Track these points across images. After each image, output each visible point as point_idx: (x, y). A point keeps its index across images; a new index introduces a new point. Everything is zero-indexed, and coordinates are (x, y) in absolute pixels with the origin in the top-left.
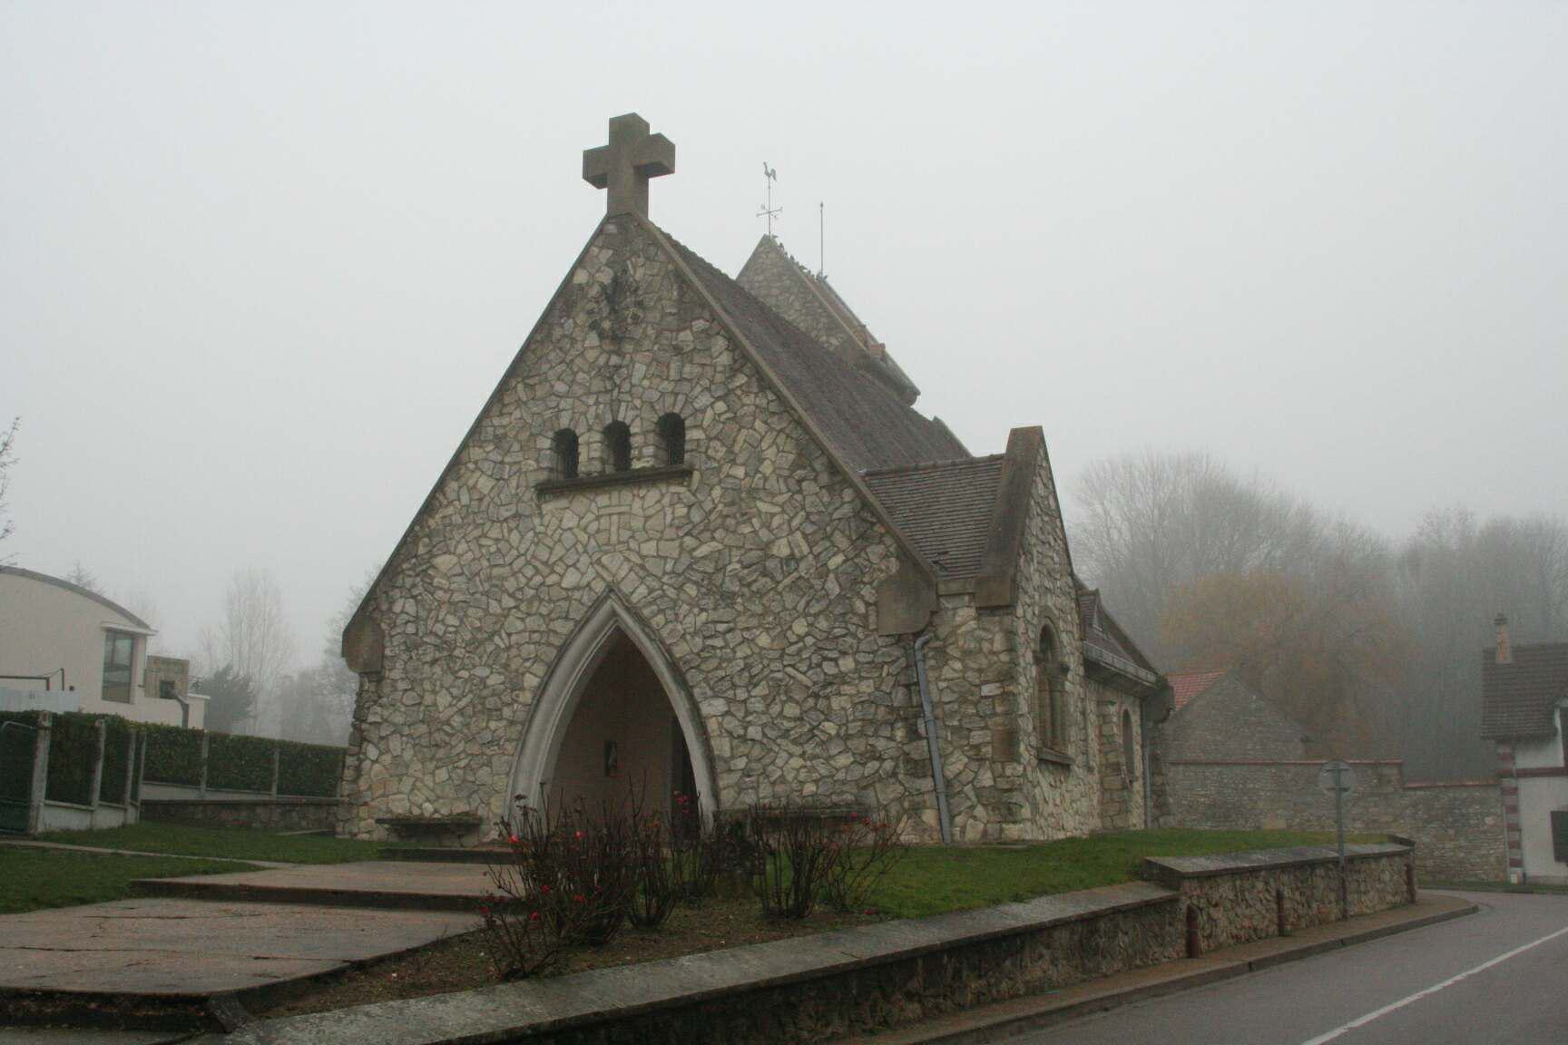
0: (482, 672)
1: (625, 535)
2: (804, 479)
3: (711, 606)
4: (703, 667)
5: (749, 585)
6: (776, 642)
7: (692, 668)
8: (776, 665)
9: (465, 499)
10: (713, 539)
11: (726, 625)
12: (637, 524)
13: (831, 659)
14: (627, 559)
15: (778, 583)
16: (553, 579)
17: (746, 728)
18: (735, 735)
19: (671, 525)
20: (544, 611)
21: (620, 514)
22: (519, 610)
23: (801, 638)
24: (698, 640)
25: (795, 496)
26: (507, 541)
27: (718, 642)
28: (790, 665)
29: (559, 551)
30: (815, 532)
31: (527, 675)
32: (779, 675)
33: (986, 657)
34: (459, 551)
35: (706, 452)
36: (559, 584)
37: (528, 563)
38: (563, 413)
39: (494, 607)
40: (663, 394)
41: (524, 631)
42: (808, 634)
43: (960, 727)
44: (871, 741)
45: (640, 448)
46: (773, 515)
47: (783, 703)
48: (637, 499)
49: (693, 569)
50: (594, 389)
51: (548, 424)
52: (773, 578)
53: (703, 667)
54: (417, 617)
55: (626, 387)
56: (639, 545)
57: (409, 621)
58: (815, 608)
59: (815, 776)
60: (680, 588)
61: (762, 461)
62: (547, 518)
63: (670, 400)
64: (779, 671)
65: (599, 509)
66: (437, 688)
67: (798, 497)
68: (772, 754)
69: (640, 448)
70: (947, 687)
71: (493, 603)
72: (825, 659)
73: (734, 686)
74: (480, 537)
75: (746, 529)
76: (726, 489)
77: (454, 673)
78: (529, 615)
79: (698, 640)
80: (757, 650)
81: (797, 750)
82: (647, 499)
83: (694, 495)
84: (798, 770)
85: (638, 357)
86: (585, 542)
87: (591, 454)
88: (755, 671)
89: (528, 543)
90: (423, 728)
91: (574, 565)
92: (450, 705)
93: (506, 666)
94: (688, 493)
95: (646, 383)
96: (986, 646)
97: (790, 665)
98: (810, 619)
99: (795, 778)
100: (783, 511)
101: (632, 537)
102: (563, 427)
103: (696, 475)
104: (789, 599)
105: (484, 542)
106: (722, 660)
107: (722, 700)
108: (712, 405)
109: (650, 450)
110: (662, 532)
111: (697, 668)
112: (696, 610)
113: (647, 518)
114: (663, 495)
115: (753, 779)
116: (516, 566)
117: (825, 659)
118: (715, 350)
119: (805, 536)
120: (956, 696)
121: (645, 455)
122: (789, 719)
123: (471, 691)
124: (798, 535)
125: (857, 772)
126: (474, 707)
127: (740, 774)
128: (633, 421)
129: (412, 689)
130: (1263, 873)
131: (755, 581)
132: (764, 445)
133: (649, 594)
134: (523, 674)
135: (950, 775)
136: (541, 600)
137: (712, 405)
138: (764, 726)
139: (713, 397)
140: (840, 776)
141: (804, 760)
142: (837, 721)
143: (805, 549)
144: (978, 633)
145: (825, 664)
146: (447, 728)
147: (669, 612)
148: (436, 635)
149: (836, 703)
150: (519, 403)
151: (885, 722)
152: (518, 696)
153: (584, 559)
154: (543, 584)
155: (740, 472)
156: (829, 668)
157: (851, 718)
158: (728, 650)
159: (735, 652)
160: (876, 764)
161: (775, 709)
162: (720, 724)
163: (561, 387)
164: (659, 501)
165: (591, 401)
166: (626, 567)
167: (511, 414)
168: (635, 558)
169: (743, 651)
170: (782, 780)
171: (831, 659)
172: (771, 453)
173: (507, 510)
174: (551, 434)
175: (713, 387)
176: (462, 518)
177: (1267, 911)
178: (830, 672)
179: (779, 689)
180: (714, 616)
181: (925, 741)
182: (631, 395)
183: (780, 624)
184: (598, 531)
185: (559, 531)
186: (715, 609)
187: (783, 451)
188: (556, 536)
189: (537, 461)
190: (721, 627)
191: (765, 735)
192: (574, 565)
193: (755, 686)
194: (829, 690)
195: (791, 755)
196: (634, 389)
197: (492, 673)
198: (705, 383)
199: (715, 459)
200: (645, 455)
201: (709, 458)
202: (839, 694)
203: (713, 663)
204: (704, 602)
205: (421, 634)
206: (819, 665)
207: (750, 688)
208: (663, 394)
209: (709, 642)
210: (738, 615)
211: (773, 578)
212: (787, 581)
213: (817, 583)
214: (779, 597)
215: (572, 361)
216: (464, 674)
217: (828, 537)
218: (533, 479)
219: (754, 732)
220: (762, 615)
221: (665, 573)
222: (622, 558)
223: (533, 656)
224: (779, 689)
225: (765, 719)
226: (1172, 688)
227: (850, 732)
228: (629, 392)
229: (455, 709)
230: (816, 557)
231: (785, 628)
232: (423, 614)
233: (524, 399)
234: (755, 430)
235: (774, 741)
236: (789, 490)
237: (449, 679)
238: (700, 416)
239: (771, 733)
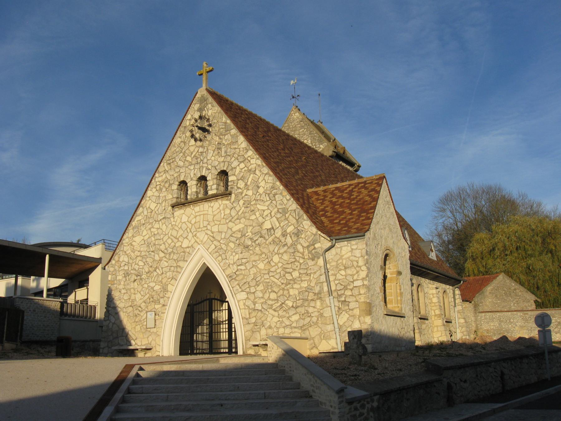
0: (152, 284)
1: (206, 223)
2: (276, 194)
3: (240, 252)
4: (237, 278)
5: (255, 241)
6: (266, 266)
7: (233, 279)
8: (266, 276)
9: (145, 213)
10: (240, 223)
11: (245, 260)
12: (210, 218)
13: (289, 273)
14: (206, 234)
15: (267, 240)
16: (178, 244)
17: (255, 305)
18: (251, 308)
19: (223, 218)
20: (175, 257)
21: (204, 214)
22: (166, 258)
23: (276, 264)
24: (235, 267)
25: (273, 202)
26: (161, 229)
27: (242, 267)
28: (272, 276)
29: (181, 232)
30: (281, 217)
31: (169, 285)
32: (268, 281)
33: (355, 268)
34: (143, 235)
35: (237, 186)
36: (181, 246)
37: (169, 238)
38: (182, 174)
39: (157, 258)
40: (219, 163)
41: (168, 266)
42: (279, 262)
43: (345, 301)
44: (306, 308)
45: (211, 186)
46: (264, 211)
47: (270, 293)
48: (210, 208)
49: (232, 236)
50: (193, 162)
51: (176, 179)
52: (264, 238)
53: (237, 278)
54: (128, 263)
55: (205, 160)
56: (211, 227)
57: (126, 265)
58: (282, 251)
59: (284, 325)
60: (227, 245)
61: (258, 187)
62: (176, 218)
63: (222, 164)
64: (268, 279)
65: (195, 213)
66: (136, 292)
67: (274, 202)
68: (266, 315)
69: (211, 186)
70: (339, 283)
71: (157, 255)
72: (287, 273)
73: (250, 287)
74: (151, 228)
75: (253, 217)
76: (245, 201)
77: (142, 286)
78: (170, 259)
79: (235, 267)
80: (258, 270)
81: (276, 314)
82: (216, 205)
83: (232, 204)
84: (276, 323)
85: (210, 148)
86: (190, 228)
87: (193, 188)
88: (257, 280)
89: (169, 229)
90: (131, 309)
91: (186, 238)
92: (141, 299)
93: (161, 282)
94: (230, 204)
95: (213, 158)
96: (355, 263)
97: (272, 276)
98: (280, 256)
99: (275, 326)
100: (268, 209)
101: (208, 224)
102: (181, 180)
103: (233, 195)
104: (271, 248)
105: (152, 230)
106: (244, 275)
107: (245, 292)
108: (239, 165)
109: (215, 187)
110: (220, 221)
111: (235, 279)
112: (234, 254)
113: (214, 216)
114: (220, 205)
115: (258, 327)
116: (164, 240)
117: (287, 273)
118: (239, 142)
119: (277, 219)
120: (343, 287)
121: (213, 188)
122: (272, 300)
123: (148, 293)
124: (274, 219)
125: (301, 323)
126: (150, 299)
127: (253, 325)
128: (208, 174)
129: (127, 293)
130: (493, 364)
131: (257, 240)
132: (260, 181)
133: (215, 248)
134: (167, 285)
135: (341, 323)
136: (174, 253)
137: (239, 165)
138: (262, 303)
139: (239, 162)
140: (294, 325)
141: (279, 318)
142: (292, 300)
143: (278, 225)
144: (351, 258)
145: (287, 275)
146: (140, 309)
147: (223, 255)
148: (135, 270)
149: (292, 292)
150: (165, 171)
151: (312, 300)
152: (166, 294)
153: (190, 235)
154: (175, 246)
155: (250, 193)
156: (288, 277)
157: (298, 298)
158: (247, 271)
159: (250, 272)
160: (309, 319)
161: (266, 296)
162: (244, 304)
163: (181, 163)
164: (219, 208)
165: (192, 167)
166: (206, 236)
167: (162, 176)
168: (209, 232)
169: (254, 270)
170: (270, 327)
171: (289, 273)
172: (262, 184)
173: (161, 216)
174: (177, 183)
175: (239, 157)
176: (145, 221)
177: (496, 381)
178: (289, 278)
179: (269, 286)
180: (241, 256)
181: (330, 308)
182: (207, 164)
183: (267, 258)
184: (195, 223)
185: (181, 223)
186: (241, 253)
187: (267, 183)
188: (179, 226)
189: (172, 195)
190: (244, 261)
191: (263, 308)
192: (186, 238)
193: (258, 285)
194: (288, 286)
195: (274, 316)
196: (208, 161)
197: (156, 285)
198: (236, 156)
199: (240, 188)
200: (213, 188)
201: (238, 188)
202: (293, 288)
203: (241, 277)
204: (237, 250)
205: (130, 269)
206: (284, 276)
207: (256, 287)
208: (219, 163)
209: (239, 267)
210: (251, 255)
211: (264, 238)
212: (271, 239)
213: (283, 239)
214: (267, 246)
215: (185, 152)
216: (146, 286)
217: (286, 219)
218: (170, 203)
219: (259, 307)
220: (261, 255)
221: (221, 239)
222: (205, 233)
223: (171, 277)
224: (269, 286)
225: (262, 300)
226: (309, 355)
227: (298, 305)
228: (206, 163)
229: (142, 300)
230: (282, 228)
231: (270, 260)
232: (131, 261)
233: (167, 170)
234: (256, 174)
235: (266, 310)
236: (270, 199)
237: (140, 288)
238: (234, 170)
239: (265, 307)
